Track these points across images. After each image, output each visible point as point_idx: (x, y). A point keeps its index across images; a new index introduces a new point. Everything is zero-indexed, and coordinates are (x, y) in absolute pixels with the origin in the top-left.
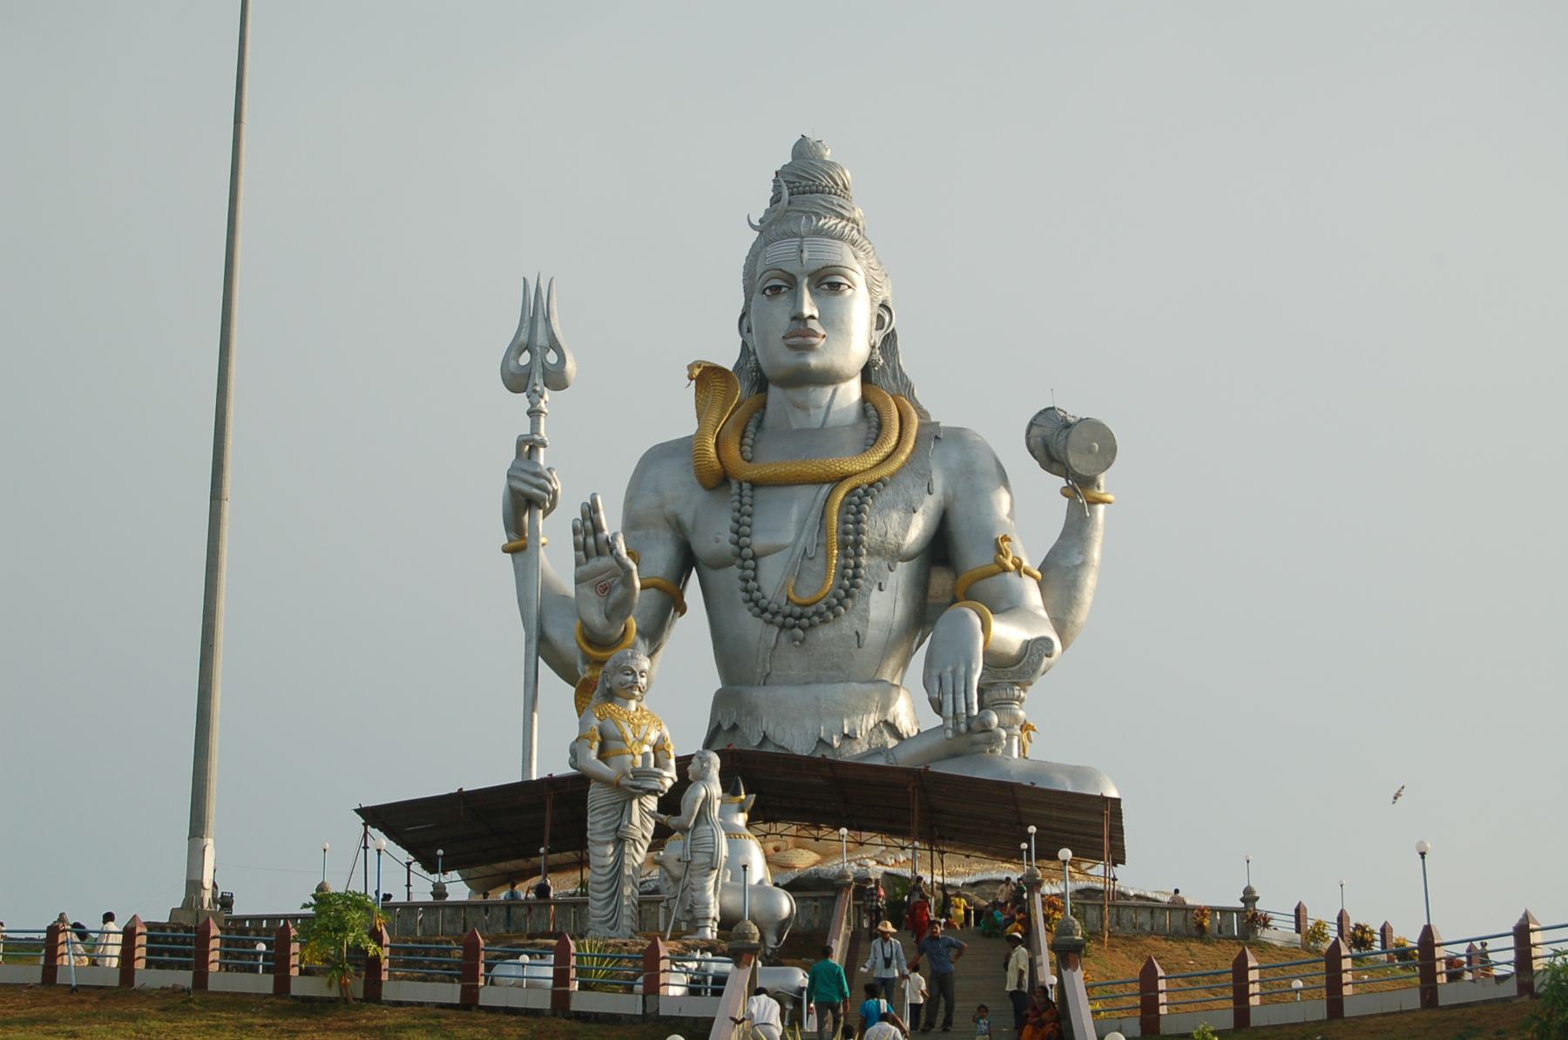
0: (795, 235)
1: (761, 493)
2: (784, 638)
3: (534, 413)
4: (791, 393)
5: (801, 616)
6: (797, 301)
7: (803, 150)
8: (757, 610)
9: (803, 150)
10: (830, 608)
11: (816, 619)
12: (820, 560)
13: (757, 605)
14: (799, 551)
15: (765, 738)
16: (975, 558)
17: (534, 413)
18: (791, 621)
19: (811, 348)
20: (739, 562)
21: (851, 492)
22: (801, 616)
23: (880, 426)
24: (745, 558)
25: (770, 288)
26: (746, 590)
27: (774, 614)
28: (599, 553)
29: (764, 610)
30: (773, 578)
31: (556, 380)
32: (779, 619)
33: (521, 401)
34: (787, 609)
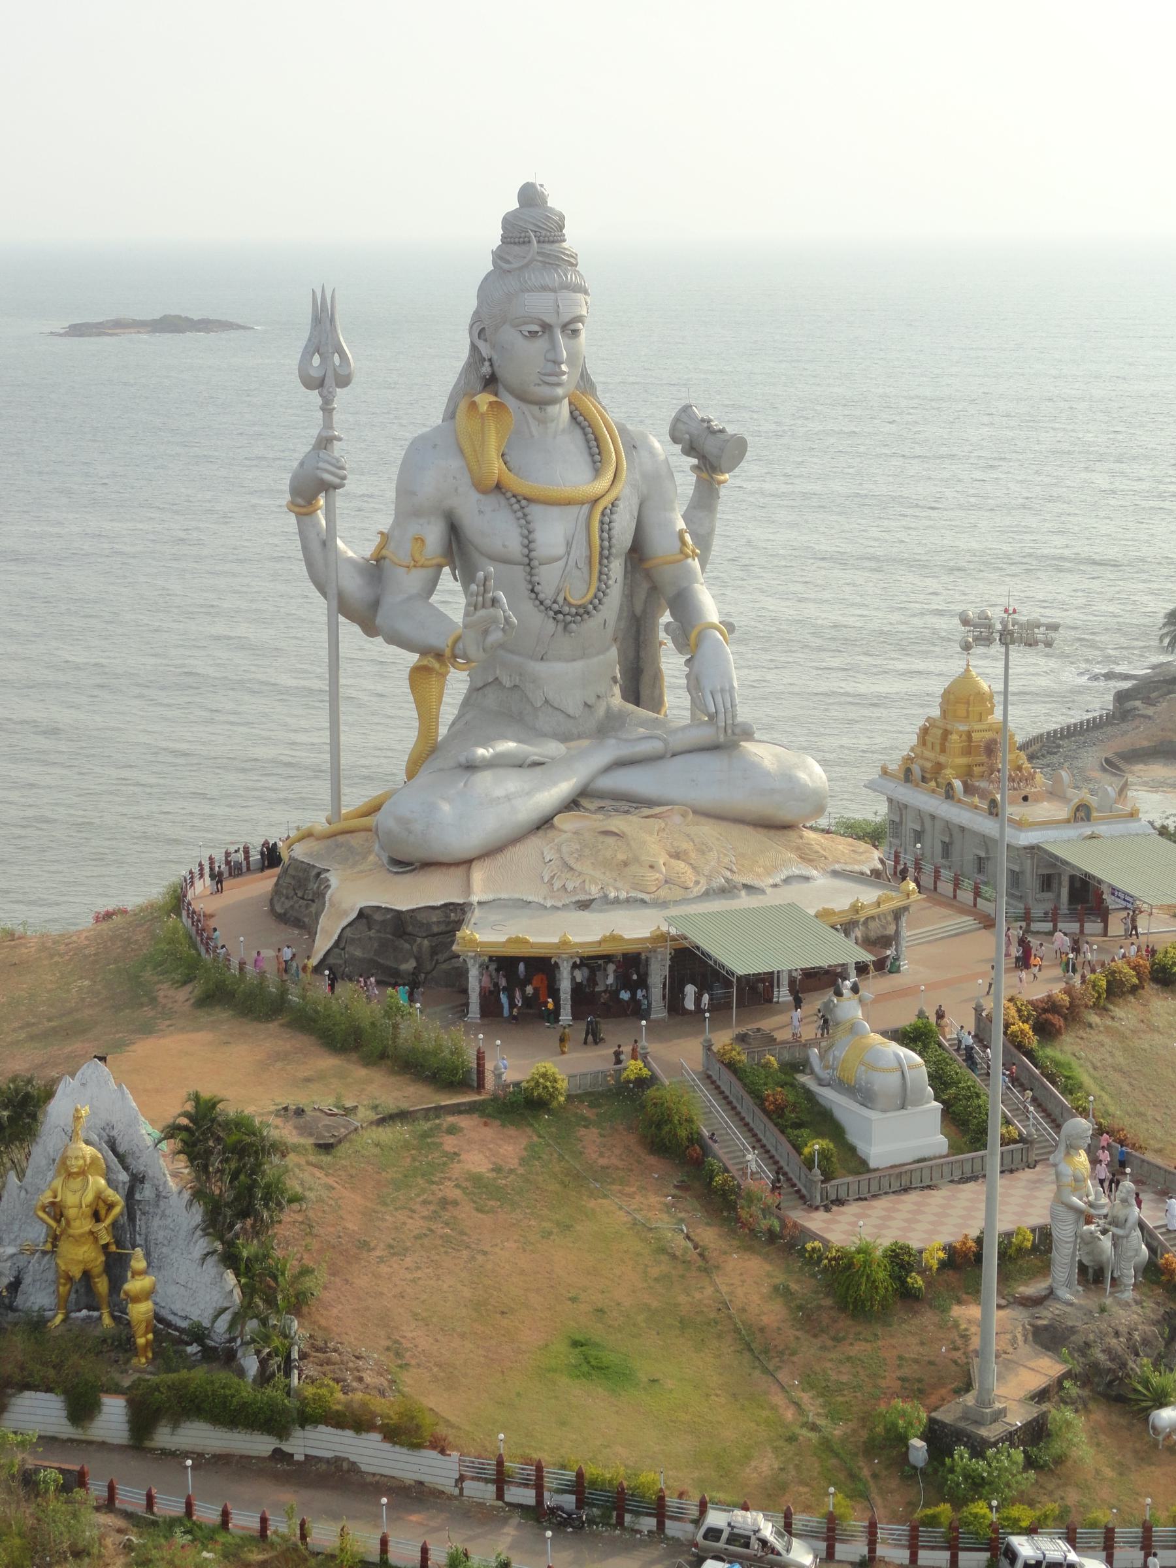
0: (553, 290)
1: (535, 511)
2: (560, 627)
3: (327, 409)
4: (535, 409)
5: (577, 614)
6: (554, 346)
7: (530, 196)
8: (542, 607)
9: (530, 196)
10: (595, 608)
11: (586, 616)
12: (585, 570)
13: (542, 603)
14: (571, 563)
15: (547, 701)
16: (661, 545)
17: (327, 409)
18: (569, 618)
19: (559, 384)
20: (528, 569)
21: (603, 514)
22: (577, 614)
23: (596, 439)
24: (529, 563)
25: (529, 332)
26: (532, 591)
27: (557, 613)
28: (483, 606)
29: (548, 608)
30: (549, 579)
31: (344, 381)
32: (560, 617)
33: (314, 397)
34: (566, 609)
